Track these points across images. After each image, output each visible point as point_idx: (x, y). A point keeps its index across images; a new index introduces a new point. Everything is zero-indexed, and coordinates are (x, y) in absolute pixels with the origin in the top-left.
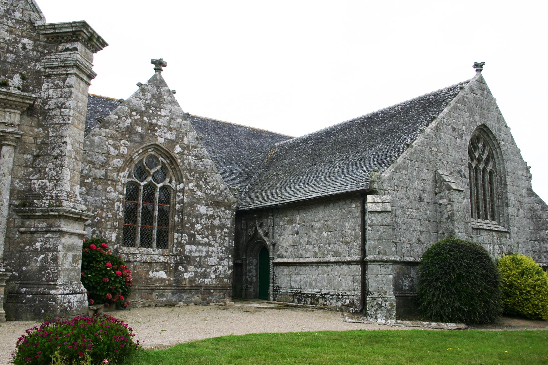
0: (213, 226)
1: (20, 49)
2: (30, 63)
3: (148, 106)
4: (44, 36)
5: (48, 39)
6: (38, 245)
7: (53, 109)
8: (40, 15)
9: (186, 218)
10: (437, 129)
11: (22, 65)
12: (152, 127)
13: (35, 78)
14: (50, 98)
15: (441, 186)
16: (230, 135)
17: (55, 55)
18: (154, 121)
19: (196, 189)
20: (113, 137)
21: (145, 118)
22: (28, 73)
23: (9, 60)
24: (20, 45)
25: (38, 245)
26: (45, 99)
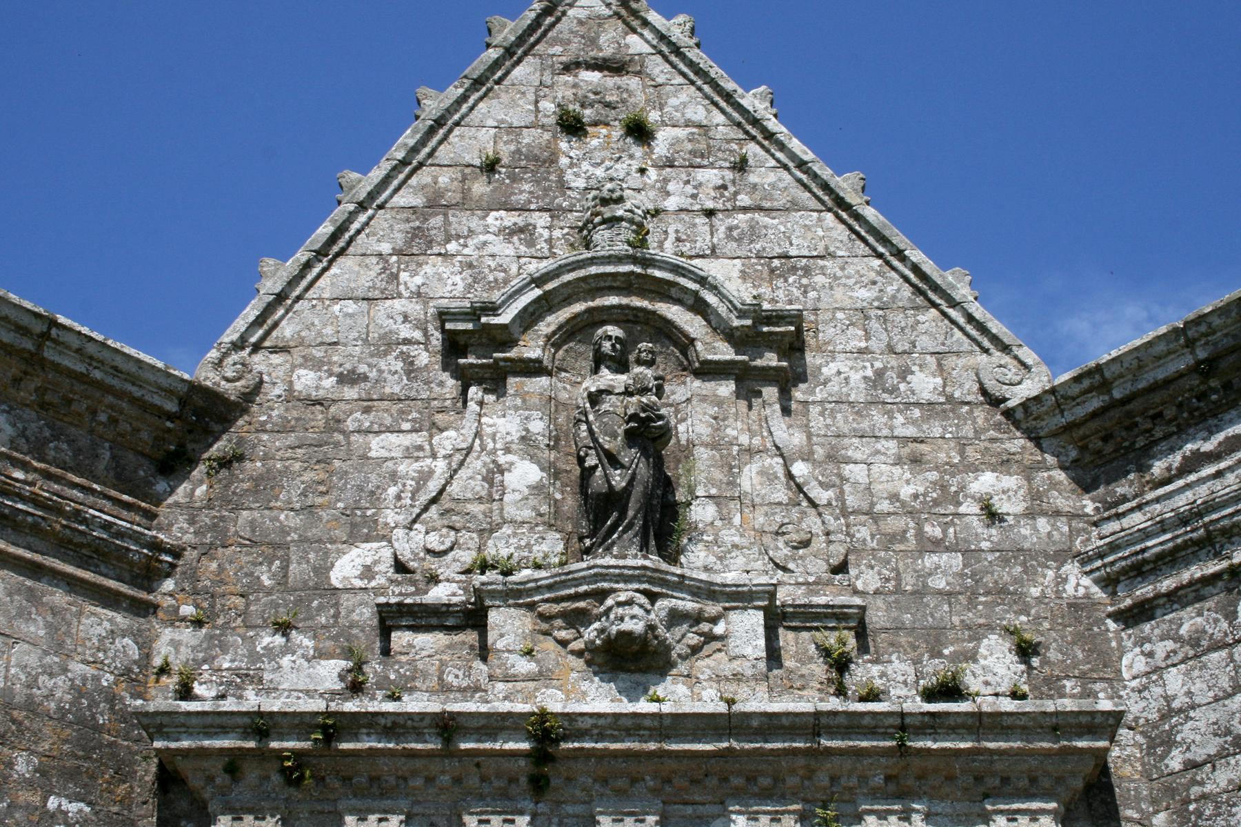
1: (975, 522)
2: (1035, 573)
4: (1065, 437)
5: (1083, 449)
7: (1211, 760)
8: (1016, 358)
11: (1002, 591)
13: (1078, 638)
14: (1180, 711)
17: (1139, 507)
22: (1037, 620)
23: (939, 583)
24: (970, 508)
26: (1155, 726)
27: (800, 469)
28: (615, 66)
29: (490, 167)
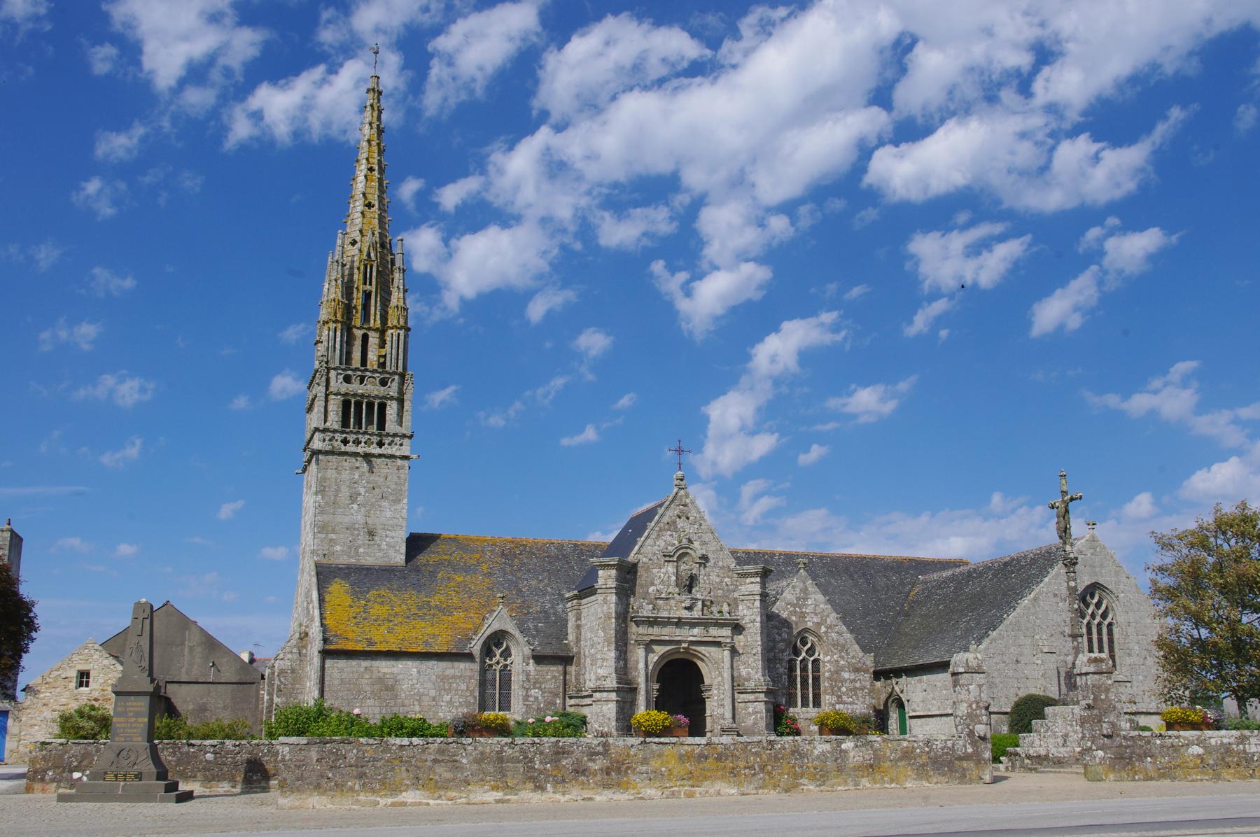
0: (855, 688)
3: (798, 599)
6: (750, 710)
9: (834, 684)
10: (1035, 599)
12: (803, 615)
15: (1037, 650)
16: (864, 574)
18: (804, 610)
19: (839, 659)
20: (776, 627)
21: (797, 609)
24: (724, 584)
25: (750, 710)
27: (705, 578)
28: (685, 505)
29: (668, 523)
